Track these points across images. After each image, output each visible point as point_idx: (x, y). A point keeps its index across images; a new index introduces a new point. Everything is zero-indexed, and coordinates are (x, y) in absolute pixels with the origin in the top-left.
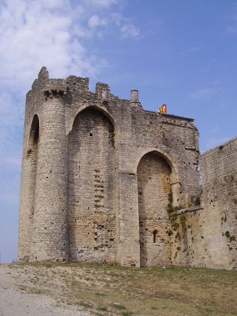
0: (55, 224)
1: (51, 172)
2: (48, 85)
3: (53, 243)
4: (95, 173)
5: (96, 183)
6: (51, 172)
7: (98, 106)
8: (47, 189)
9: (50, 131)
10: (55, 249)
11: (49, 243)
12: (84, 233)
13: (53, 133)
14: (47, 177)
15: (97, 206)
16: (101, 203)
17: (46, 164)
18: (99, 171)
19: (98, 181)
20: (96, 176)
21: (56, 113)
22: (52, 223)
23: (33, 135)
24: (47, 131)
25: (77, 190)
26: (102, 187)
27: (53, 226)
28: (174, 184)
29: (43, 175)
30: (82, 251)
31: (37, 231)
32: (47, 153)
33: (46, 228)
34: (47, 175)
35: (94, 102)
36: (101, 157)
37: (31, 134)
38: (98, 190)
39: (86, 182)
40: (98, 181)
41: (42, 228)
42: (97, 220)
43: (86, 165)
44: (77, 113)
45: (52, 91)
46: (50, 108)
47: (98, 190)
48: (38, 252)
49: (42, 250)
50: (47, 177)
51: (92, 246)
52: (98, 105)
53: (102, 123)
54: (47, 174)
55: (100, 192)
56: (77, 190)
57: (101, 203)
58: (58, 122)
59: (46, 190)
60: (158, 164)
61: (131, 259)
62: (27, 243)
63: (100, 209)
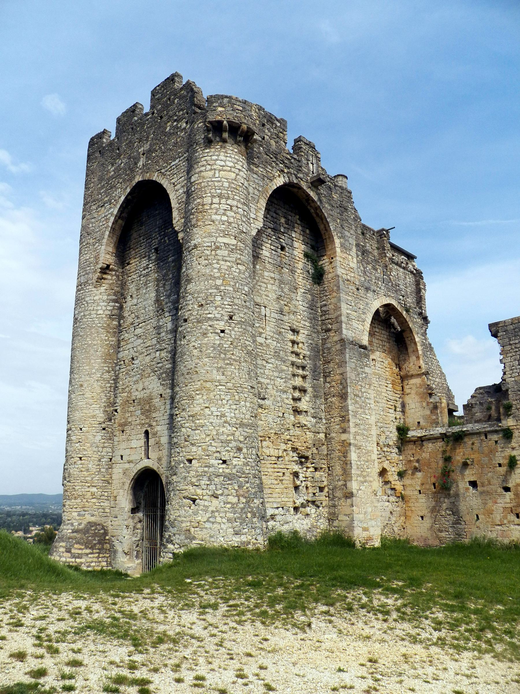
0: (245, 450)
1: (231, 318)
2: (220, 109)
3: (244, 500)
4: (290, 336)
5: (294, 358)
6: (231, 318)
7: (305, 188)
8: (224, 359)
9: (224, 218)
10: (249, 515)
11: (235, 500)
12: (276, 474)
13: (230, 223)
14: (223, 331)
15: (297, 411)
16: (303, 405)
17: (218, 298)
18: (298, 332)
19: (297, 354)
20: (293, 342)
21: (235, 180)
22: (240, 449)
23: (118, 233)
24: (214, 217)
25: (262, 371)
26: (303, 368)
27: (242, 456)
28: (412, 376)
29: (210, 323)
30: (273, 517)
31: (200, 470)
32: (219, 269)
33: (224, 462)
34: (221, 325)
35: (297, 178)
36: (300, 302)
37: (113, 229)
38: (298, 375)
39: (277, 355)
40: (297, 354)
41: (215, 462)
42: (297, 445)
43: (276, 316)
44: (270, 193)
45: (230, 123)
46: (223, 163)
47: (298, 375)
48: (208, 525)
49: (219, 519)
50: (223, 331)
51: (291, 505)
52: (304, 185)
53: (300, 228)
54: (222, 323)
55: (300, 379)
56: (262, 371)
57: (303, 405)
58: (239, 201)
59: (221, 364)
60: (383, 332)
61: (368, 532)
62: (94, 490)
63: (303, 419)
